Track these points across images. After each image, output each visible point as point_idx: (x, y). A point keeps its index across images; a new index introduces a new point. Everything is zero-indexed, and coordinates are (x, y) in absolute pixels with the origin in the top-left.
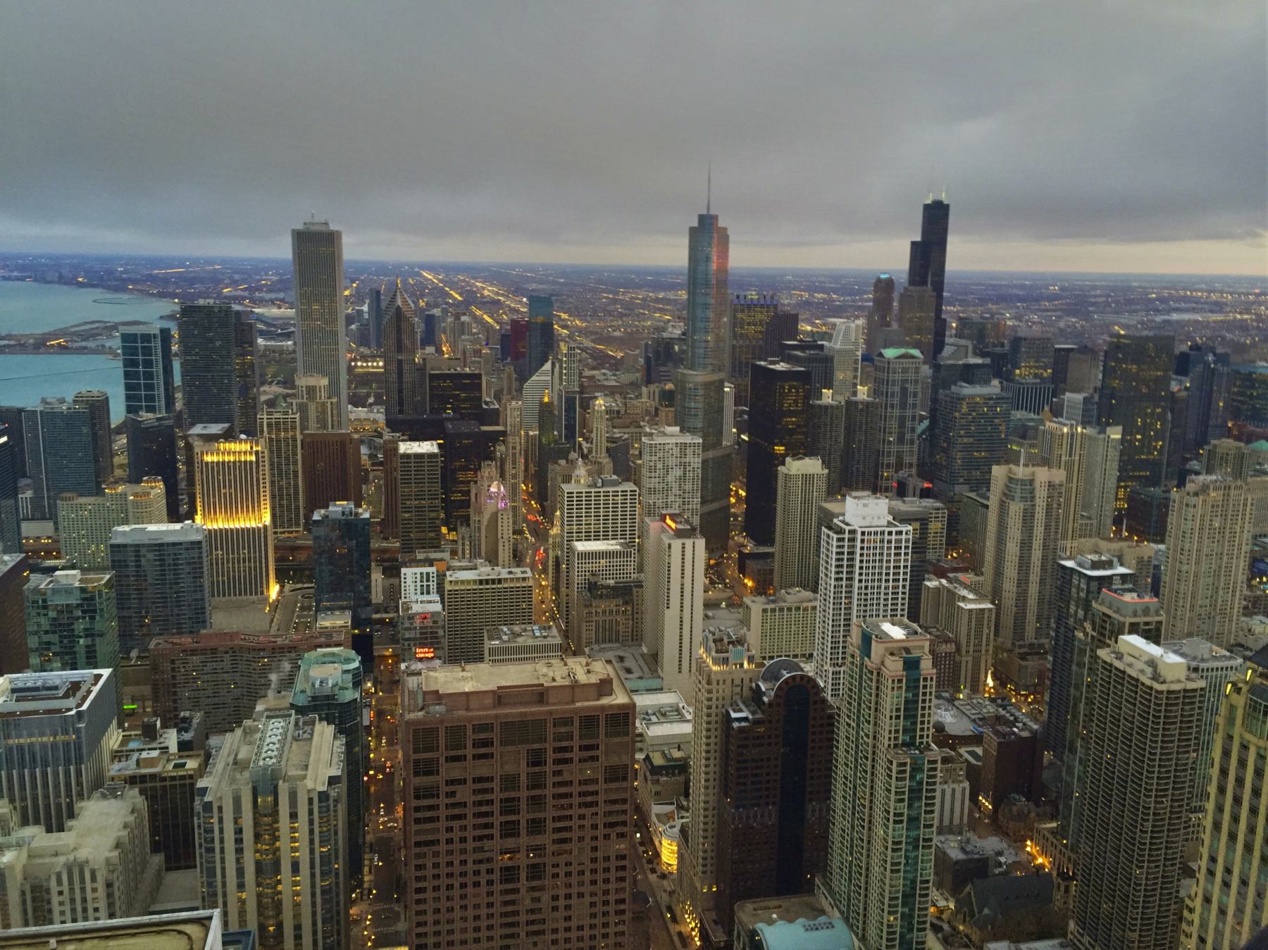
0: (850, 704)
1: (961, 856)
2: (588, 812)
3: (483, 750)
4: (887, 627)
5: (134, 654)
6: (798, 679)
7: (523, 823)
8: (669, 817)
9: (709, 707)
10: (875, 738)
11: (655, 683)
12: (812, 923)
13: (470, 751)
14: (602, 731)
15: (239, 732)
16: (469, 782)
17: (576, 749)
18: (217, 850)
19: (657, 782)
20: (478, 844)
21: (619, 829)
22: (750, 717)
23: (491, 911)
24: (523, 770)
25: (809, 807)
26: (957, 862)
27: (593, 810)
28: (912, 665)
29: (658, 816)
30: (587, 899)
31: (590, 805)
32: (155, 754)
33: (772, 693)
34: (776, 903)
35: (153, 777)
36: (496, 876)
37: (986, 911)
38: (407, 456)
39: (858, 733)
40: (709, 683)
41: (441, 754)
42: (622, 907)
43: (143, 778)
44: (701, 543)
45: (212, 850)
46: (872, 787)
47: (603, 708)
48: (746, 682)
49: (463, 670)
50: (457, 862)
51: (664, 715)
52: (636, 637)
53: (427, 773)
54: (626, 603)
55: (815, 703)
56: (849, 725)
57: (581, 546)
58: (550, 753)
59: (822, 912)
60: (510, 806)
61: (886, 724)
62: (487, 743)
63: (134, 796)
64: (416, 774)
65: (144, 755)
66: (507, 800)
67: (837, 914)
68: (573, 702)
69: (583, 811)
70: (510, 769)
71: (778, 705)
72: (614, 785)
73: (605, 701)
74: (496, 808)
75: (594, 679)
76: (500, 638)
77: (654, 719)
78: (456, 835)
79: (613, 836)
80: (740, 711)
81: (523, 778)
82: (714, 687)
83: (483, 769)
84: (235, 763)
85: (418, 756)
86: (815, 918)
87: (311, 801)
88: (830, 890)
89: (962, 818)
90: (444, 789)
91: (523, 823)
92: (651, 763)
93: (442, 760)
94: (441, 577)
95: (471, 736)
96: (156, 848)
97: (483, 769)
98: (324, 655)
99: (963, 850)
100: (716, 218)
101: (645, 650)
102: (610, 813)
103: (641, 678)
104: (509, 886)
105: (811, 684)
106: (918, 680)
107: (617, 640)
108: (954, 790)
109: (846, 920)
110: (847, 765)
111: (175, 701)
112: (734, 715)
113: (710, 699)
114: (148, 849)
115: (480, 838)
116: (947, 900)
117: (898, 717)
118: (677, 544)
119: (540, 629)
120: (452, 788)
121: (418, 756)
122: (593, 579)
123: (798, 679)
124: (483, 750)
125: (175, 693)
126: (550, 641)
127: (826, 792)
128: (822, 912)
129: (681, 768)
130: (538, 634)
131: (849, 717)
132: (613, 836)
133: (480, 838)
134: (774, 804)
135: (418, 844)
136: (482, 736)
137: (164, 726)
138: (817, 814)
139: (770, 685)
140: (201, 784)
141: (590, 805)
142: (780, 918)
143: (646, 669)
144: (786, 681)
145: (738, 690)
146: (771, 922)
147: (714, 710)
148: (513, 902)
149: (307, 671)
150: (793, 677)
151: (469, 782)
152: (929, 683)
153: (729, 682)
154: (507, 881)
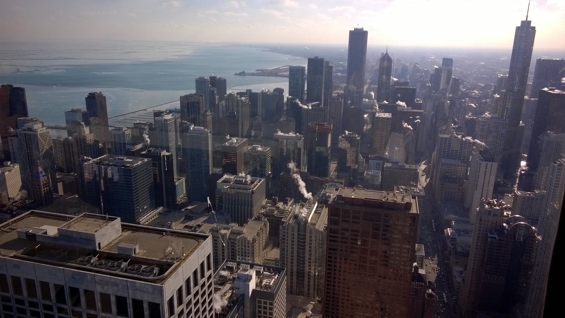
8: (461, 273)
22: (497, 237)
38: (378, 118)
40: (481, 220)
43: (269, 216)
44: (495, 165)
54: (460, 186)
57: (444, 161)
77: (462, 233)
80: (493, 234)
94: (384, 164)
100: (530, 22)
112: (489, 235)
118: (484, 164)
122: (447, 174)
129: (466, 255)
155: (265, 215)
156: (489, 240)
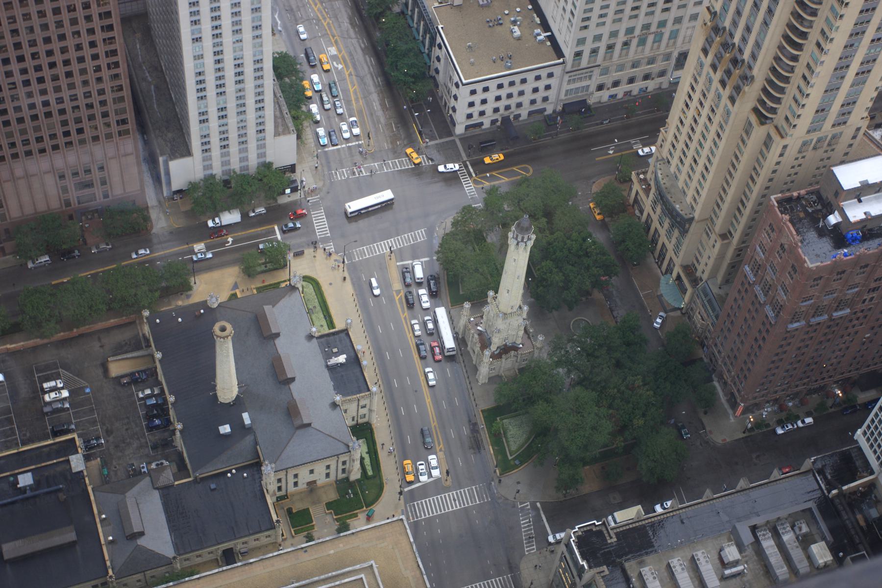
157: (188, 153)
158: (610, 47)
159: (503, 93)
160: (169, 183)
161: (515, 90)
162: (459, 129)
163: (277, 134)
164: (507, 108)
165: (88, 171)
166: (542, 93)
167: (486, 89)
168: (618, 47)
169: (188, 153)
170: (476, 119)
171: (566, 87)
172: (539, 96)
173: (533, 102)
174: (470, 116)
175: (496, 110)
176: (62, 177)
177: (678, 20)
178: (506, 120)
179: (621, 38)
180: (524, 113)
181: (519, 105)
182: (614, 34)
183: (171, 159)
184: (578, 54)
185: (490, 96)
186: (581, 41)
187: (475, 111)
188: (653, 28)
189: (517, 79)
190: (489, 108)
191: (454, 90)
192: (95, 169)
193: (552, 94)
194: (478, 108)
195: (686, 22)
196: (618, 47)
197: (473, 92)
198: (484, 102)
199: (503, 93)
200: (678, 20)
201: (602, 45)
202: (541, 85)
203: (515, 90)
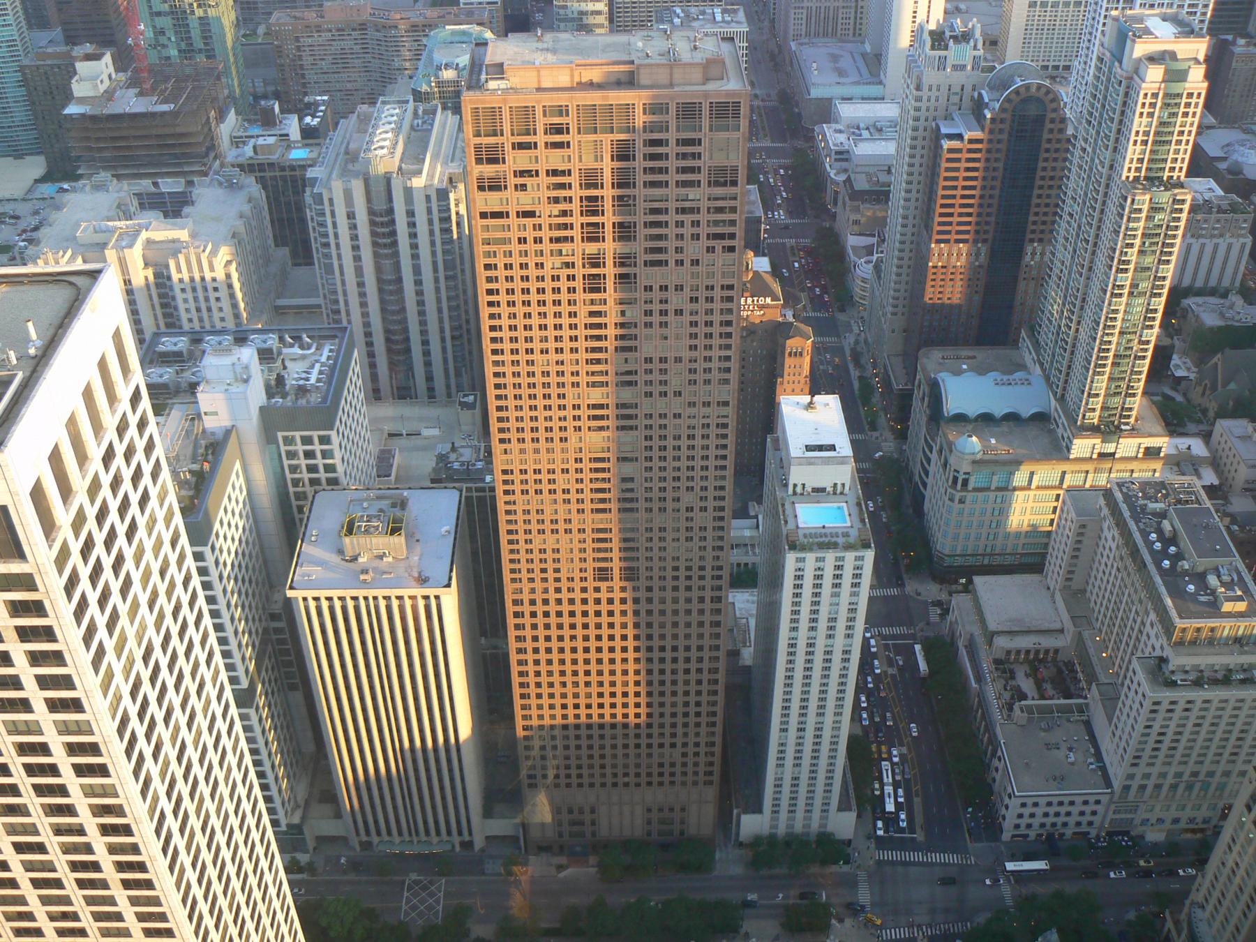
0: (1089, 123)
1: (1220, 323)
2: (688, 218)
3: (557, 138)
4: (1154, 23)
5: (261, 30)
6: (1033, 89)
7: (609, 228)
8: (869, 250)
9: (917, 119)
10: (1111, 167)
11: (874, 90)
12: (1005, 378)
13: (541, 138)
14: (706, 122)
15: (354, 117)
16: (542, 174)
17: (672, 142)
18: (333, 246)
19: (857, 210)
20: (556, 246)
21: (727, 243)
23: (573, 321)
24: (607, 166)
25: (1029, 249)
26: (1211, 329)
27: (695, 217)
28: (1176, 76)
29: (853, 248)
30: (687, 318)
31: (691, 210)
32: (271, 140)
33: (997, 106)
34: (970, 353)
35: (271, 165)
36: (578, 284)
37: (1232, 386)
39: (1093, 160)
40: (918, 88)
41: (507, 140)
42: (729, 329)
43: (261, 168)
45: (327, 245)
46: (1099, 228)
47: (706, 95)
48: (968, 89)
49: (539, 39)
50: (532, 265)
51: (880, 130)
52: (858, 34)
53: (493, 161)
55: (1052, 121)
56: (1084, 150)
58: (639, 144)
59: (1022, 367)
60: (592, 206)
61: (1133, 152)
62: (559, 130)
63: (252, 186)
64: (479, 161)
65: (261, 141)
66: (589, 199)
67: (1038, 370)
68: (671, 85)
69: (680, 217)
70: (589, 162)
71: (1002, 121)
72: (719, 191)
73: (711, 86)
74: (575, 206)
75: (699, 57)
76: (671, 22)
77: (866, 134)
78: (530, 235)
79: (719, 249)
81: (607, 177)
82: (925, 93)
83: (555, 159)
84: (347, 153)
85: (478, 140)
86: (1011, 373)
87: (428, 198)
88: (1037, 345)
89: (1234, 279)
90: (512, 181)
91: (609, 228)
92: (852, 186)
93: (508, 147)
95: (541, 123)
96: (280, 241)
97: (555, 159)
98: (454, 33)
99: (1222, 315)
101: (868, 48)
102: (716, 223)
103: (857, 83)
104: (594, 296)
105: (1051, 96)
106: (1180, 95)
107: (834, 34)
108: (1230, 246)
109: (1047, 378)
110: (1074, 199)
111: (304, 85)
112: (944, 130)
113: (917, 109)
114: (271, 242)
115: (558, 240)
116: (1188, 369)
117: (1145, 143)
119: (724, 12)
120: (520, 181)
121: (478, 140)
123: (1033, 89)
124: (557, 138)
125: (303, 76)
126: (735, 28)
127: (1046, 235)
128: (1022, 367)
129: (881, 196)
130: (719, 18)
131: (1086, 140)
132: (719, 249)
133: (558, 240)
134: (985, 241)
135: (487, 242)
136: (556, 120)
137: (282, 111)
138: (1038, 257)
139: (996, 95)
140: (311, 173)
141: (691, 210)
142: (971, 369)
143: (864, 71)
144: (1017, 92)
145: (956, 99)
146: (958, 373)
147: (922, 123)
148: (598, 314)
149: (431, 52)
150: (1028, 87)
151: (542, 174)
152: (1194, 101)
153: (944, 90)
154: (592, 290)
155: (248, 168)
156: (946, 144)
157: (758, 809)
158: (1158, 787)
159: (1051, 810)
160: (738, 834)
161: (1063, 810)
162: (1006, 836)
163: (839, 810)
164: (1054, 825)
165: (672, 810)
166: (1088, 818)
167: (1036, 805)
168: (1165, 788)
169: (758, 809)
170: (1022, 831)
171: (1110, 815)
172: (1085, 820)
173: (1078, 824)
174: (1017, 826)
175: (1043, 825)
176: (649, 810)
177: (1227, 774)
178: (1050, 836)
179: (1170, 780)
180: (1068, 833)
181: (1065, 824)
182: (1163, 775)
183: (746, 812)
184: (1127, 788)
185: (1039, 811)
186: (1131, 777)
187: (1023, 822)
188: (1201, 777)
189: (1066, 800)
190: (1036, 822)
191: (1007, 800)
192: (677, 808)
193: (1097, 820)
194: (1026, 820)
195: (1234, 777)
196: (1165, 788)
197: (1024, 805)
198: (1032, 815)
199: (1051, 810)
200: (1227, 774)
201: (1150, 783)
202: (1088, 809)
203: (1063, 810)
